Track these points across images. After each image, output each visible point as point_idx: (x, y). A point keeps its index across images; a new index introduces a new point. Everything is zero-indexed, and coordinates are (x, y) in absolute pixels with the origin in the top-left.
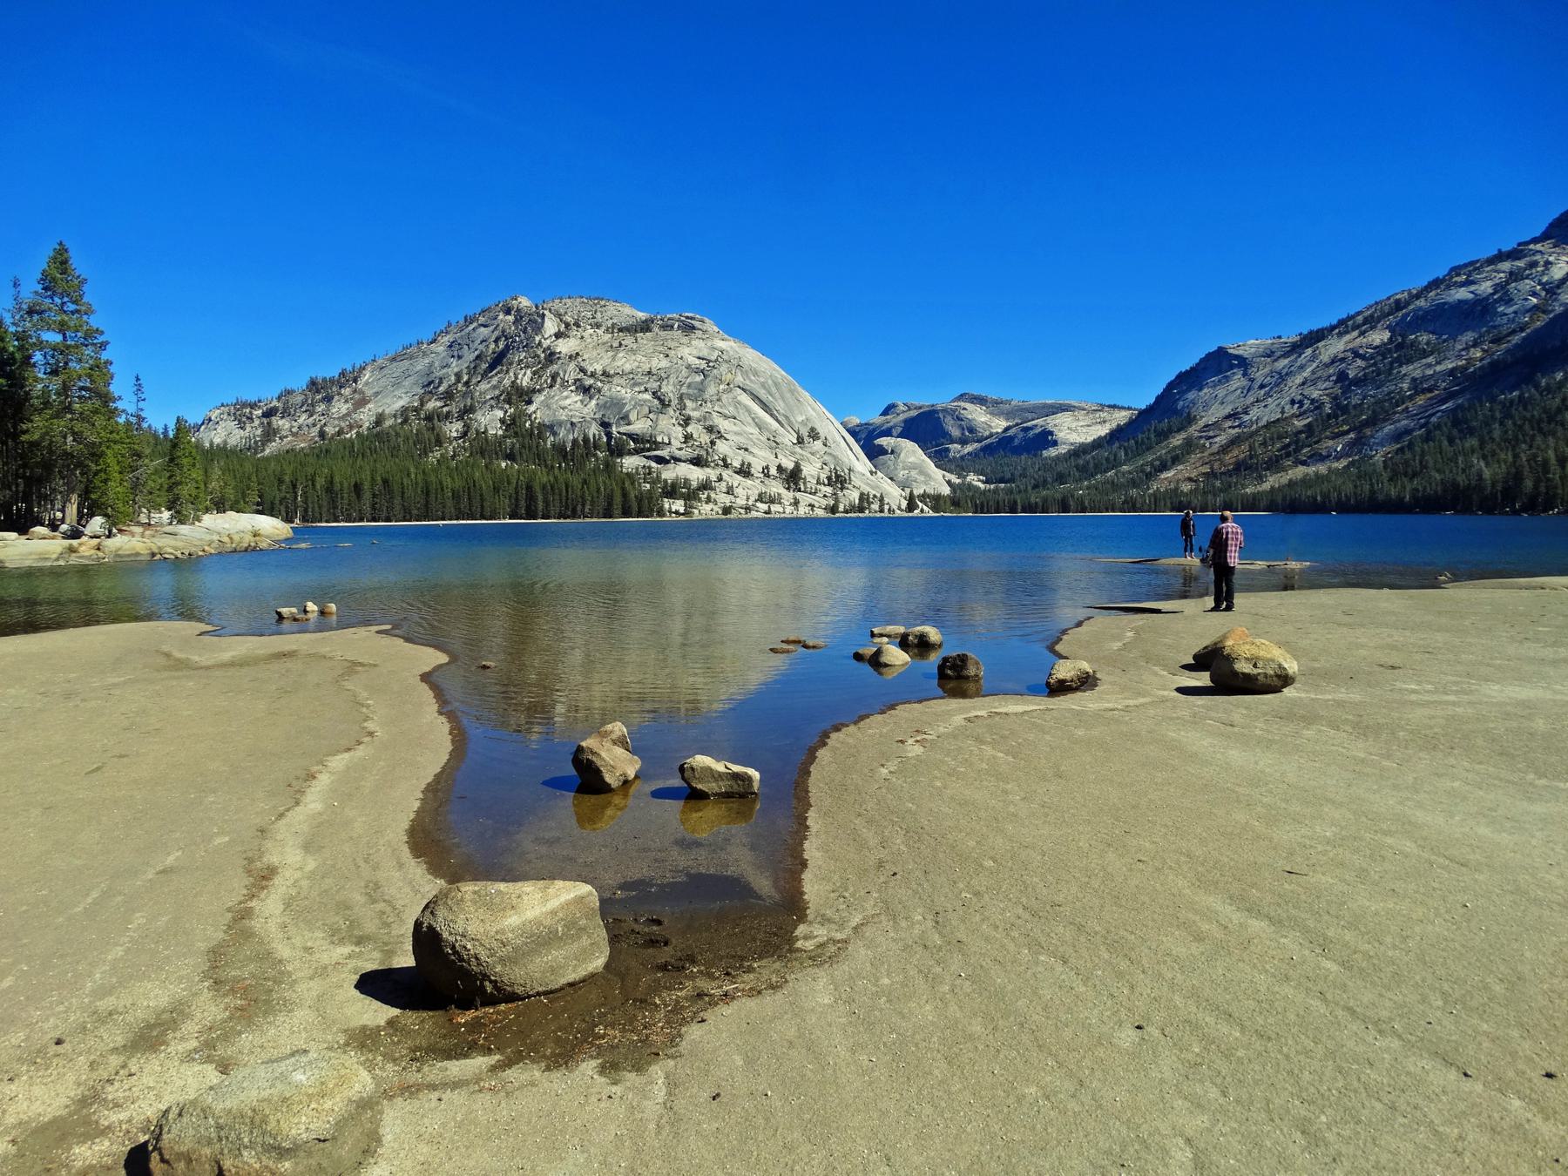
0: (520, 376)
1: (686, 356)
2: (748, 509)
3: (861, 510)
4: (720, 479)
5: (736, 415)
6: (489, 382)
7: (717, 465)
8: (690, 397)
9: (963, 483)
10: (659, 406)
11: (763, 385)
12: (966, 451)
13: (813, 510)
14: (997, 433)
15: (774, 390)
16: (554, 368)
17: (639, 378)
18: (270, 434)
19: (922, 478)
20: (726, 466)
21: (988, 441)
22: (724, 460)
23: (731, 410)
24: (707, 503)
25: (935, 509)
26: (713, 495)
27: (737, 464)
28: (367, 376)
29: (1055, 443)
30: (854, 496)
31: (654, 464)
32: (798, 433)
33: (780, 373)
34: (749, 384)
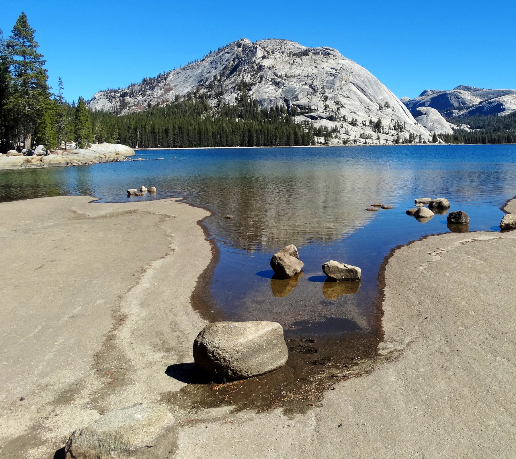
0: (245, 77)
1: (325, 67)
2: (355, 141)
3: (410, 142)
4: (342, 127)
5: (350, 96)
6: (230, 80)
7: (341, 120)
8: (327, 87)
9: (460, 129)
10: (313, 92)
11: (363, 82)
12: (461, 113)
13: (387, 142)
14: (476, 105)
15: (368, 84)
16: (261, 73)
17: (302, 78)
18: (124, 105)
19: (440, 127)
20: (345, 120)
21: (472, 108)
22: (344, 118)
23: (347, 94)
24: (335, 138)
25: (446, 141)
26: (338, 135)
27: (350, 120)
28: (171, 77)
29: (504, 110)
30: (407, 135)
31: (310, 120)
32: (380, 105)
33: (371, 76)
34: (356, 81)
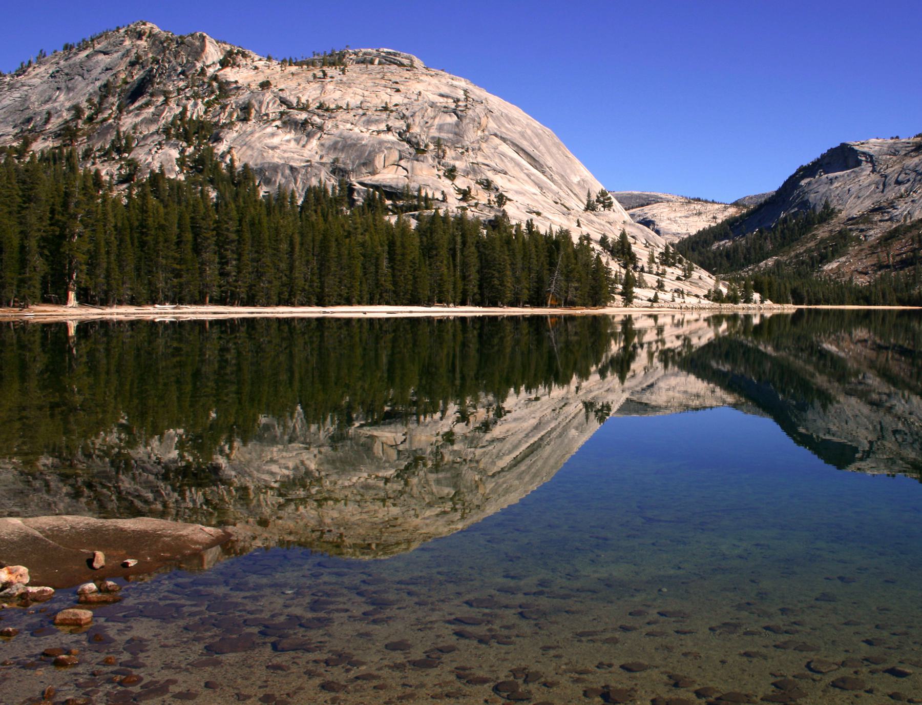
11: (523, 135)
15: (536, 141)
33: (536, 124)
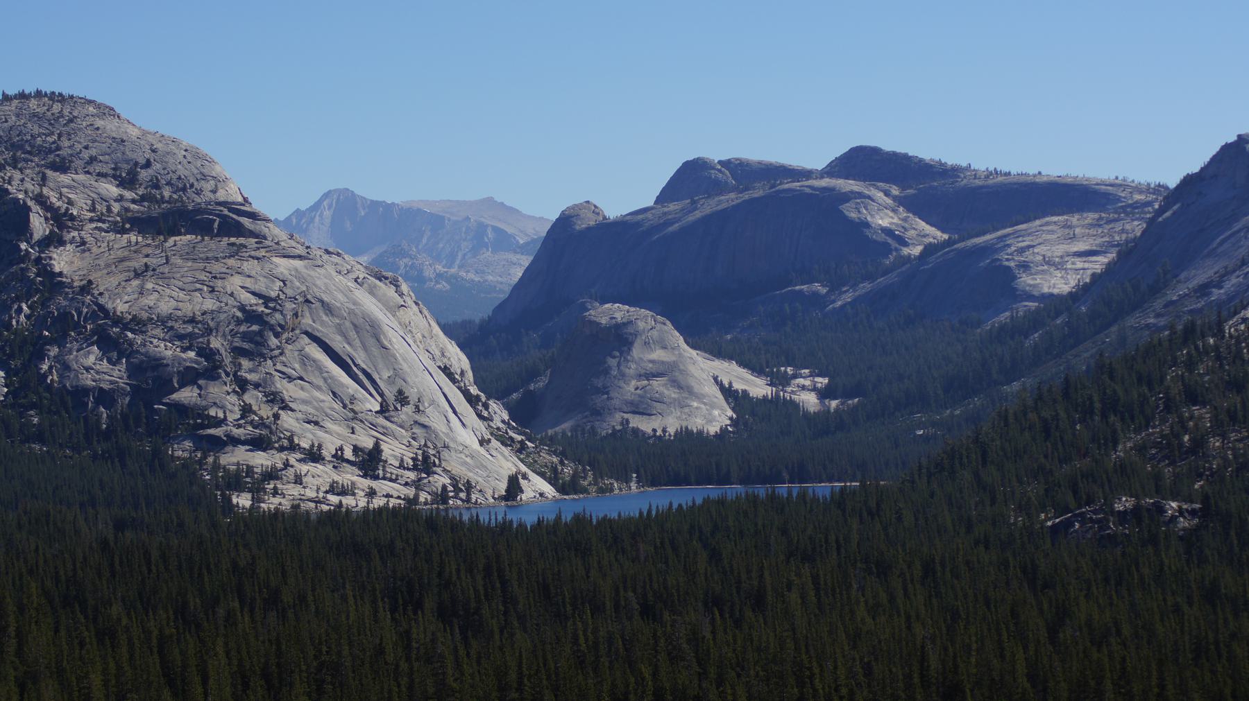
15: (353, 334)
22: (291, 439)
